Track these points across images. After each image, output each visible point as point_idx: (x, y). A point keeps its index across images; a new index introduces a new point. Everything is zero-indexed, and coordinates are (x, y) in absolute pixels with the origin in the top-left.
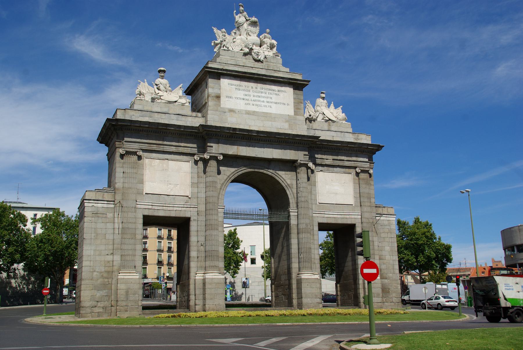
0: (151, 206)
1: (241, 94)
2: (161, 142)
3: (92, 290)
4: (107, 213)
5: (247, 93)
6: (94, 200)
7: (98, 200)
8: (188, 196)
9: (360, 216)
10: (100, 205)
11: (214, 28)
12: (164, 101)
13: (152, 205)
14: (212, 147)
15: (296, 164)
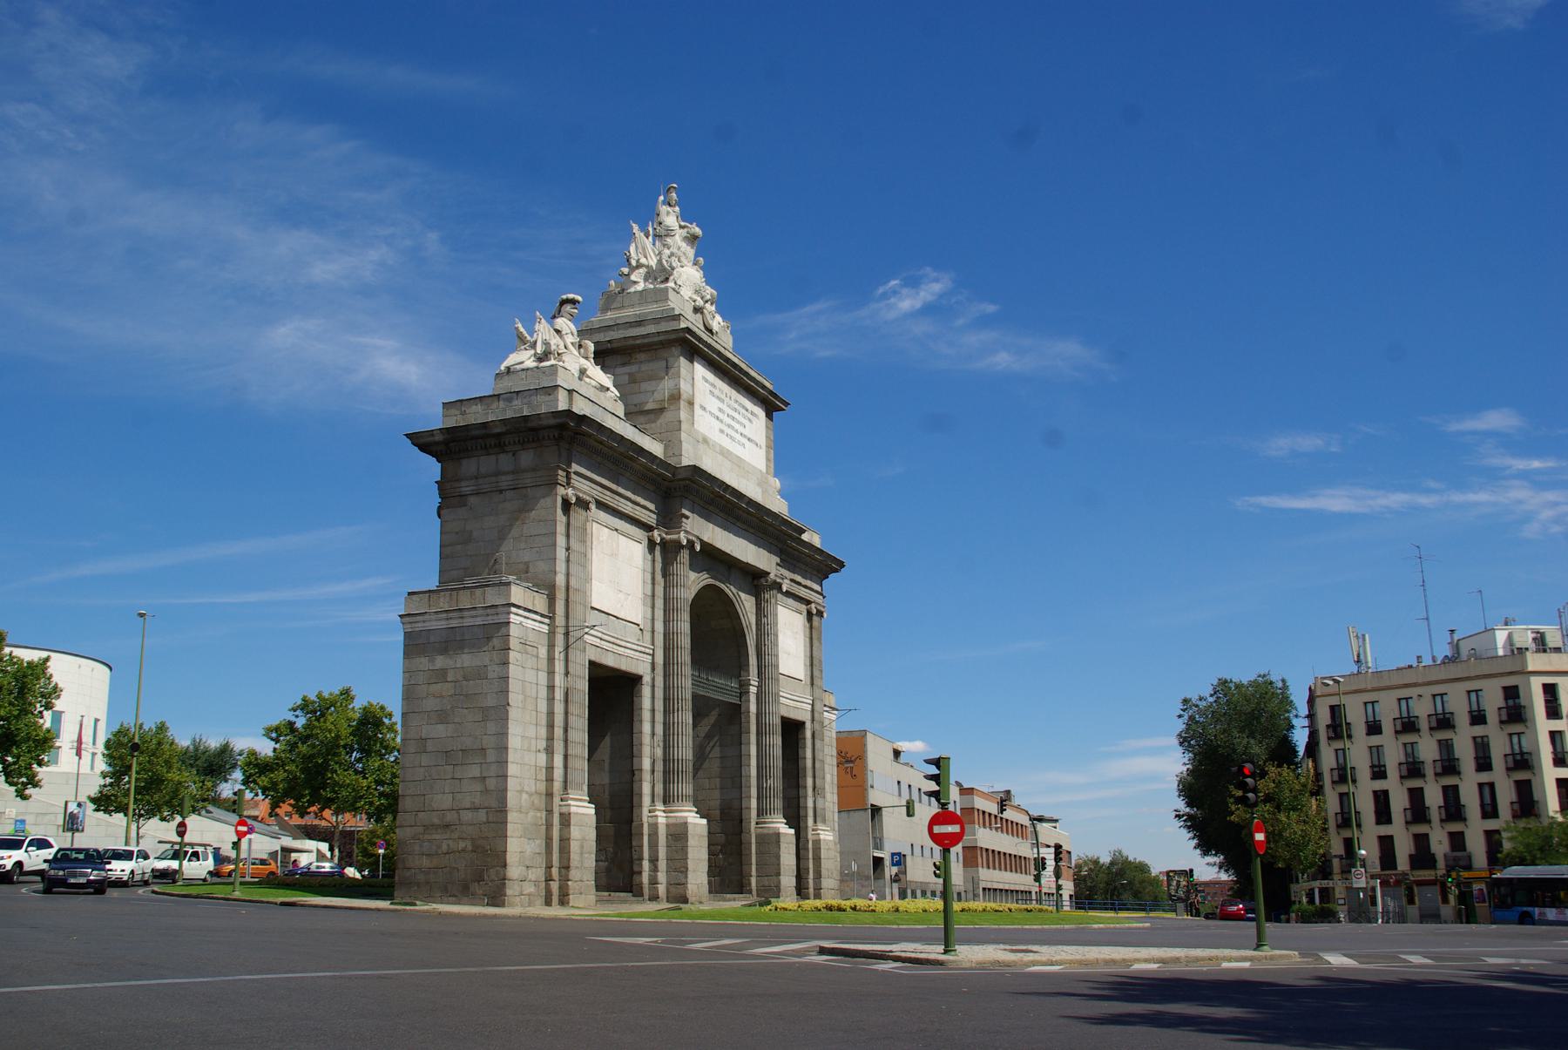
0: (599, 640)
1: (713, 405)
2: (614, 486)
3: (521, 837)
4: (539, 647)
5: (721, 405)
6: (526, 610)
7: (529, 611)
8: (638, 625)
9: (810, 706)
10: (530, 624)
11: (634, 225)
12: (594, 383)
13: (601, 639)
14: (687, 518)
15: (763, 580)
